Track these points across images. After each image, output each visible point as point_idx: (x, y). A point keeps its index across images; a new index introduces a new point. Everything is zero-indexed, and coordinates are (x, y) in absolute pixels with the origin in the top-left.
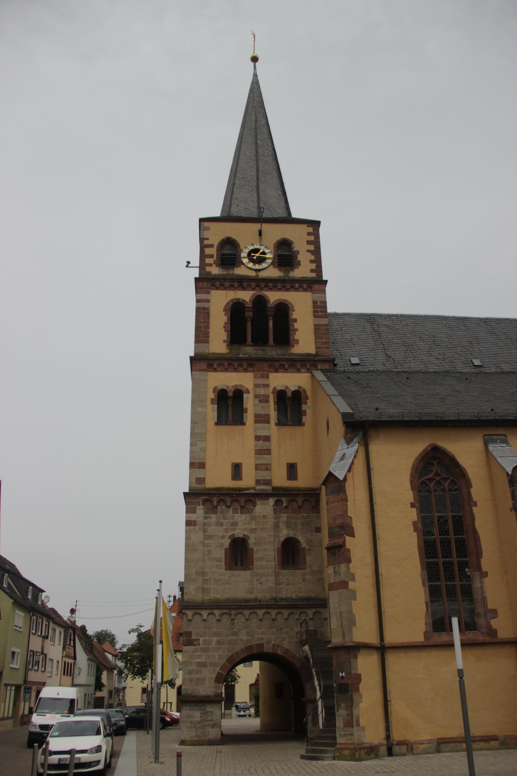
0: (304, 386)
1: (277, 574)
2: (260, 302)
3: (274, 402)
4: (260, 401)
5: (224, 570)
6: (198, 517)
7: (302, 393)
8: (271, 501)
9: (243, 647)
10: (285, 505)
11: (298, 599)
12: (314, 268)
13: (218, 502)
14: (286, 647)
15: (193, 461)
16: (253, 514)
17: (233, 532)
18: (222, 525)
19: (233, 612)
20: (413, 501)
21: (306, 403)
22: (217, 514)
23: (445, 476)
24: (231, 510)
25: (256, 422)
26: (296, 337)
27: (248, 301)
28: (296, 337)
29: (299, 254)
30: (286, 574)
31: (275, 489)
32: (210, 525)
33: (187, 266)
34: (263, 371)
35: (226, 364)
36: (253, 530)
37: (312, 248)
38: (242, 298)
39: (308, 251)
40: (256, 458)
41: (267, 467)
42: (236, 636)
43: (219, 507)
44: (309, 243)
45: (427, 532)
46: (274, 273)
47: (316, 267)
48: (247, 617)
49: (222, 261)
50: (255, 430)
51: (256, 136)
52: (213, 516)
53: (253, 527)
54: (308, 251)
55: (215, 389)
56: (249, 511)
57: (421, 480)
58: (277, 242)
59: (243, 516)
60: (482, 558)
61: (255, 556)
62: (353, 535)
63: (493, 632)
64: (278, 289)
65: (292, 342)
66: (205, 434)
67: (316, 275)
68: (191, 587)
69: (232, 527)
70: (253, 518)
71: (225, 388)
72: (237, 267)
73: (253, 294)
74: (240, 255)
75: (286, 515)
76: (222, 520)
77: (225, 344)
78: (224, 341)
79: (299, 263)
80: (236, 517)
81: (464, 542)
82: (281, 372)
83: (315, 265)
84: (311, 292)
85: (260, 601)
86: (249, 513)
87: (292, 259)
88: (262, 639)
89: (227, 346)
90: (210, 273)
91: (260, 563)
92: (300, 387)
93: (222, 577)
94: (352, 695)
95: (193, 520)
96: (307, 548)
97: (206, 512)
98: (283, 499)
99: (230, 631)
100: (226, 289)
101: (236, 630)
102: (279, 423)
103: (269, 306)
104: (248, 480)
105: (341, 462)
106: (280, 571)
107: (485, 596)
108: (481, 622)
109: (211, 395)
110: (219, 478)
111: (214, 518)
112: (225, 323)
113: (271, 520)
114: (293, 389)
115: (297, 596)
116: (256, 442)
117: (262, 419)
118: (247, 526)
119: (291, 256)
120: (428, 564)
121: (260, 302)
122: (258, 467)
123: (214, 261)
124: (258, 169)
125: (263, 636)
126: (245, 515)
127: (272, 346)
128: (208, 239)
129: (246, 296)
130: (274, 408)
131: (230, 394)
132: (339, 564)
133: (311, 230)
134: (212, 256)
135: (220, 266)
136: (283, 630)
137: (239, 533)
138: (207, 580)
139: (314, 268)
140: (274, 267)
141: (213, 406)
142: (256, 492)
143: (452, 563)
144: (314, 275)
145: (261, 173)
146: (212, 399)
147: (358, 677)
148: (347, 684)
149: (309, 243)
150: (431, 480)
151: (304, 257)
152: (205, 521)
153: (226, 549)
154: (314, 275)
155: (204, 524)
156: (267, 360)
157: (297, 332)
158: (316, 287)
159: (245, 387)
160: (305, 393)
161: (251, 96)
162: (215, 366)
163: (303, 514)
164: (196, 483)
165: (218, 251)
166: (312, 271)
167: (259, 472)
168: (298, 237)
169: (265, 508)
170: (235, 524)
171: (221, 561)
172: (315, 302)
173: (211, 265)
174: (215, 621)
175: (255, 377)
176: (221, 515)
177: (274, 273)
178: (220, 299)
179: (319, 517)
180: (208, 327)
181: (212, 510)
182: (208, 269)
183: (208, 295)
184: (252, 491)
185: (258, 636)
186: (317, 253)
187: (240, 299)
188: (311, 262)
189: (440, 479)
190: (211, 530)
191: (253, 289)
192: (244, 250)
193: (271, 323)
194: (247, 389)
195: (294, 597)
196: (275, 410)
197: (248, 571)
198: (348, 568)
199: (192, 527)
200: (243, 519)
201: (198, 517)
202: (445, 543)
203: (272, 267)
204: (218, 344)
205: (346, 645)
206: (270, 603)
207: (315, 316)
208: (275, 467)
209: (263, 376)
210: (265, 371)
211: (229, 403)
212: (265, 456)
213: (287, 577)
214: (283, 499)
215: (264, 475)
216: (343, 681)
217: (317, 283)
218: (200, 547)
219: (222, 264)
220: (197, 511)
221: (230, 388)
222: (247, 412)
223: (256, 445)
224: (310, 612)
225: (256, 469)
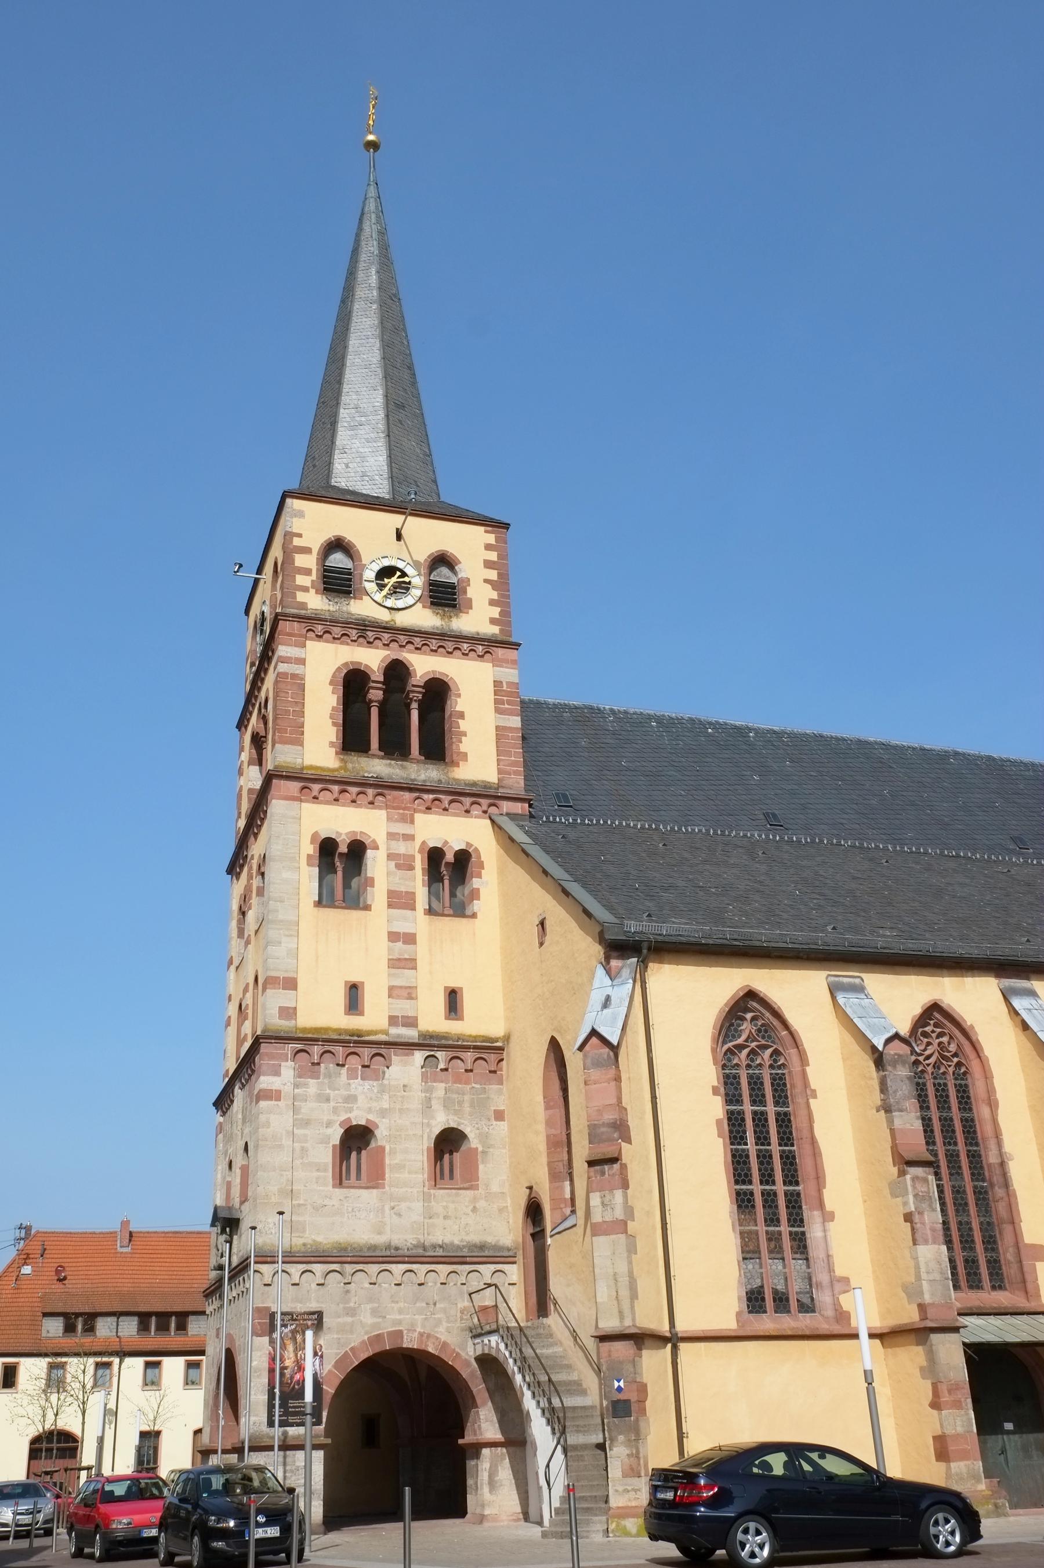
1: (426, 1198)
2: (397, 672)
4: (398, 867)
5: (330, 1187)
8: (419, 1056)
9: (366, 1338)
10: (442, 1066)
11: (464, 1247)
12: (497, 616)
14: (443, 1338)
16: (385, 1082)
17: (349, 1115)
18: (328, 1100)
19: (349, 1268)
20: (716, 1084)
21: (479, 876)
23: (763, 1042)
25: (390, 906)
27: (376, 669)
28: (463, 747)
30: (444, 1199)
31: (424, 1035)
34: (404, 809)
36: (383, 1113)
38: (364, 662)
39: (486, 581)
41: (410, 993)
42: (353, 1315)
45: (735, 1138)
46: (422, 617)
47: (500, 614)
48: (374, 1280)
52: (312, 1082)
53: (386, 1105)
54: (486, 581)
55: (315, 835)
56: (379, 1076)
57: (726, 1047)
59: (367, 1084)
60: (825, 1187)
61: (387, 1161)
62: (629, 1141)
63: (843, 1316)
65: (455, 757)
67: (501, 630)
68: (270, 1220)
69: (346, 1105)
72: (355, 598)
74: (361, 575)
75: (443, 1085)
76: (328, 1091)
77: (334, 750)
78: (332, 744)
80: (353, 1086)
81: (794, 1157)
82: (436, 813)
83: (499, 609)
84: (493, 661)
85: (397, 1249)
86: (377, 1080)
88: (400, 1322)
89: (337, 753)
90: (303, 605)
91: (397, 1175)
93: (327, 1202)
94: (637, 1420)
95: (274, 1088)
96: (480, 1149)
98: (438, 1054)
99: (341, 1306)
101: (352, 1305)
103: (414, 681)
104: (374, 1018)
105: (605, 1011)
106: (432, 1191)
107: (830, 1253)
108: (823, 1298)
109: (309, 849)
111: (312, 1086)
112: (333, 709)
113: (417, 1095)
115: (462, 1241)
117: (400, 901)
118: (375, 1105)
119: (453, 586)
120: (738, 1193)
121: (397, 672)
125: (402, 1317)
127: (418, 762)
131: (343, 849)
132: (611, 1190)
133: (491, 539)
134: (307, 572)
135: (323, 594)
136: (438, 1305)
137: (359, 1118)
138: (299, 1205)
139: (497, 616)
140: (424, 607)
141: (311, 868)
143: (775, 1194)
147: (643, 1389)
148: (627, 1402)
149: (488, 564)
150: (740, 1047)
152: (296, 1091)
153: (334, 1146)
154: (495, 630)
155: (294, 1098)
157: (463, 738)
160: (479, 856)
164: (280, 1017)
166: (493, 621)
170: (351, 1099)
171: (325, 1170)
173: (305, 589)
174: (314, 1286)
175: (389, 819)
176: (326, 1081)
180: (302, 714)
182: (301, 597)
183: (302, 650)
184: (383, 1038)
185: (393, 1317)
188: (492, 603)
189: (757, 1046)
190: (307, 1108)
193: (415, 715)
194: (374, 841)
195: (456, 1242)
197: (375, 1191)
198: (625, 1197)
199: (273, 1102)
200: (366, 1090)
202: (765, 1158)
203: (419, 605)
205: (627, 1332)
206: (414, 1252)
207: (498, 711)
208: (421, 993)
209: (403, 819)
213: (445, 1204)
214: (438, 1054)
215: (403, 1008)
216: (621, 1396)
218: (287, 1142)
219: (325, 589)
220: (283, 1071)
221: (343, 837)
223: (390, 949)
224: (487, 1270)
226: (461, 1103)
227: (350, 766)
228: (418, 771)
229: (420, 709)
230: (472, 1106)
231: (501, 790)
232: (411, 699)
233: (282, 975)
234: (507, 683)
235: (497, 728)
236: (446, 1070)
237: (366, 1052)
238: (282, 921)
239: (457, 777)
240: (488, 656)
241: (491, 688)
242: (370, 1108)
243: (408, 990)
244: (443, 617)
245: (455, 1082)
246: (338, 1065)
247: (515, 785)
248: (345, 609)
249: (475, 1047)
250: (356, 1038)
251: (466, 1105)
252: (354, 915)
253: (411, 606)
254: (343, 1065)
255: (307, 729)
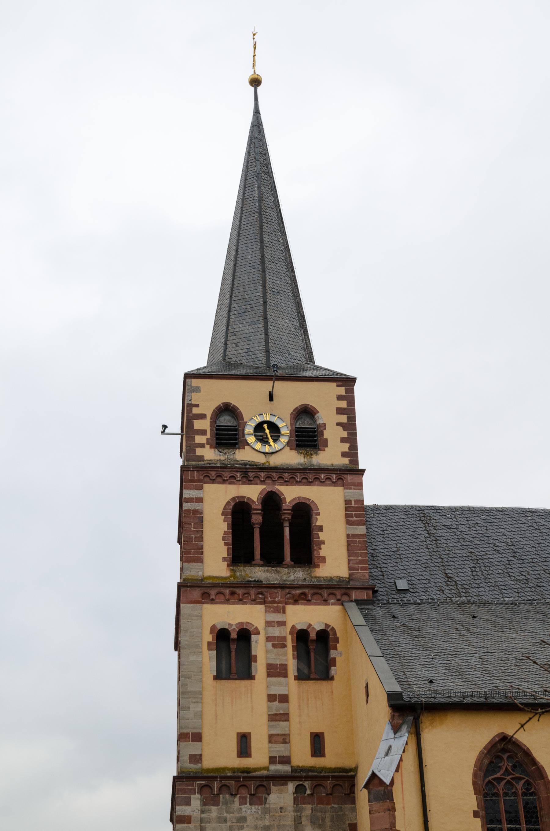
0: (332, 624)
2: (271, 500)
3: (293, 646)
4: (274, 646)
6: (194, 811)
7: (331, 633)
8: (291, 787)
10: (308, 792)
12: (347, 450)
13: (220, 789)
15: (185, 731)
16: (267, 806)
18: (225, 821)
22: (218, 805)
24: (237, 799)
25: (269, 675)
26: (322, 553)
27: (255, 500)
28: (322, 553)
29: (325, 429)
31: (294, 769)
32: (209, 822)
33: (163, 432)
35: (227, 591)
37: (343, 419)
38: (247, 496)
39: (338, 424)
40: (269, 726)
41: (285, 739)
43: (221, 796)
44: (340, 411)
47: (350, 448)
49: (217, 439)
50: (268, 687)
51: (261, 228)
52: (214, 808)
54: (338, 424)
55: (213, 628)
56: (262, 801)
58: (294, 411)
59: (254, 808)
64: (297, 482)
65: (316, 561)
66: (201, 693)
67: (350, 460)
69: (238, 824)
70: (266, 811)
71: (227, 627)
72: (239, 448)
73: (263, 490)
74: (244, 430)
76: (225, 815)
77: (226, 563)
78: (224, 559)
79: (325, 444)
80: (244, 810)
82: (302, 604)
83: (348, 445)
84: (343, 485)
86: (261, 804)
87: (315, 436)
89: (228, 566)
90: (201, 458)
92: (327, 625)
95: (186, 814)
97: (204, 804)
98: (307, 784)
100: (224, 482)
102: (301, 677)
103: (284, 507)
104: (259, 758)
109: (208, 637)
110: (220, 754)
111: (214, 811)
112: (225, 533)
113: (290, 814)
114: (318, 628)
116: (270, 703)
117: (276, 671)
118: (260, 823)
121: (271, 500)
122: (272, 739)
123: (207, 439)
124: (264, 287)
126: (256, 806)
127: (288, 566)
128: (197, 406)
129: (253, 492)
130: (293, 654)
131: (234, 635)
133: (342, 391)
134: (203, 432)
135: (216, 448)
139: (347, 450)
140: (291, 449)
141: (211, 652)
142: (271, 773)
144: (346, 461)
145: (269, 294)
146: (209, 643)
149: (340, 411)
151: (333, 434)
152: (203, 815)
154: (346, 461)
155: (202, 820)
156: (281, 587)
157: (322, 546)
158: (350, 478)
159: (253, 625)
160: (335, 633)
161: (252, 152)
162: (212, 597)
163: (333, 805)
164: (190, 762)
165: (213, 421)
166: (344, 454)
167: (274, 745)
168: (323, 400)
169: (282, 797)
172: (347, 502)
173: (202, 446)
175: (266, 611)
176: (224, 807)
177: (293, 458)
178: (216, 498)
179: (354, 810)
180: (201, 539)
181: (210, 800)
182: (199, 452)
183: (201, 492)
184: (265, 773)
186: (350, 426)
187: (244, 497)
188: (343, 440)
191: (263, 482)
192: (249, 423)
193: (287, 531)
194: (256, 628)
196: (293, 658)
199: (186, 825)
200: (253, 813)
201: (194, 811)
203: (288, 448)
204: (215, 562)
207: (348, 523)
208: (294, 739)
210: (279, 602)
211: (231, 647)
212: (282, 723)
214: (307, 784)
215: (280, 750)
217: (349, 473)
219: (217, 443)
220: (193, 801)
221: (234, 627)
222: (256, 661)
223: (269, 708)
225: (270, 742)
226: (323, 819)
227: (238, 574)
228: (289, 573)
229: (291, 526)
230: (332, 821)
231: (351, 583)
232: (284, 520)
233: (190, 731)
234: (355, 501)
235: (348, 536)
236: (312, 794)
237: (252, 785)
238: (190, 692)
239: (317, 575)
240: (340, 482)
241: (342, 505)
242: (256, 826)
243: (284, 737)
244: (305, 455)
245: (318, 804)
246: (232, 795)
247: (362, 578)
248: (232, 457)
249: (333, 777)
250: (245, 774)
251: (328, 820)
252: (243, 684)
253: (281, 450)
254: (236, 795)
255: (206, 550)
